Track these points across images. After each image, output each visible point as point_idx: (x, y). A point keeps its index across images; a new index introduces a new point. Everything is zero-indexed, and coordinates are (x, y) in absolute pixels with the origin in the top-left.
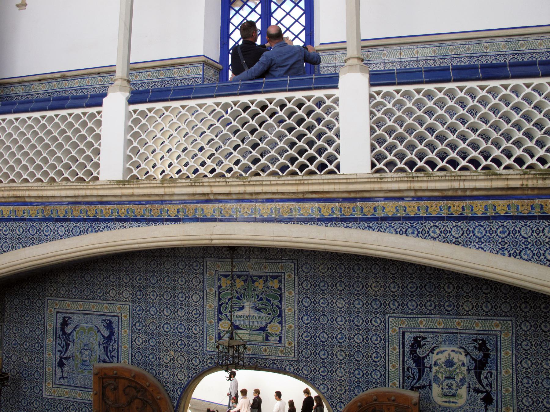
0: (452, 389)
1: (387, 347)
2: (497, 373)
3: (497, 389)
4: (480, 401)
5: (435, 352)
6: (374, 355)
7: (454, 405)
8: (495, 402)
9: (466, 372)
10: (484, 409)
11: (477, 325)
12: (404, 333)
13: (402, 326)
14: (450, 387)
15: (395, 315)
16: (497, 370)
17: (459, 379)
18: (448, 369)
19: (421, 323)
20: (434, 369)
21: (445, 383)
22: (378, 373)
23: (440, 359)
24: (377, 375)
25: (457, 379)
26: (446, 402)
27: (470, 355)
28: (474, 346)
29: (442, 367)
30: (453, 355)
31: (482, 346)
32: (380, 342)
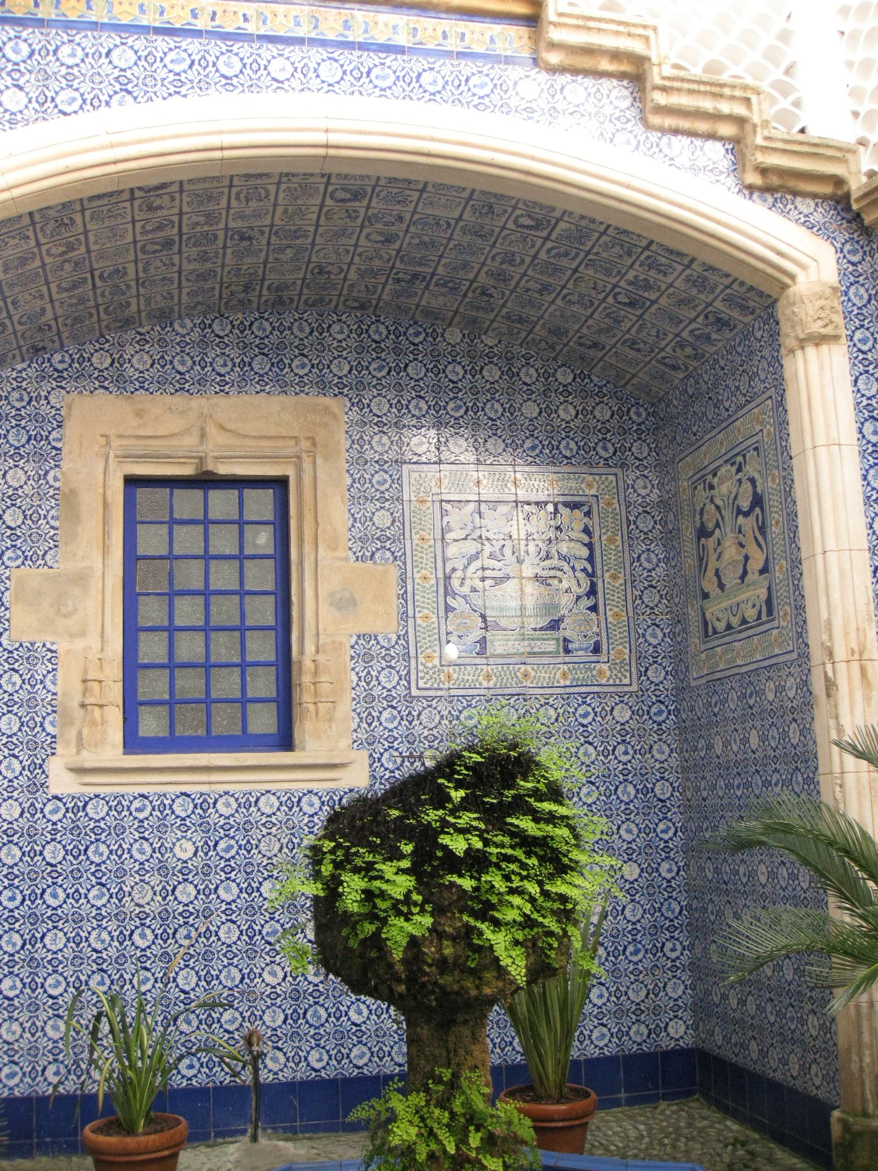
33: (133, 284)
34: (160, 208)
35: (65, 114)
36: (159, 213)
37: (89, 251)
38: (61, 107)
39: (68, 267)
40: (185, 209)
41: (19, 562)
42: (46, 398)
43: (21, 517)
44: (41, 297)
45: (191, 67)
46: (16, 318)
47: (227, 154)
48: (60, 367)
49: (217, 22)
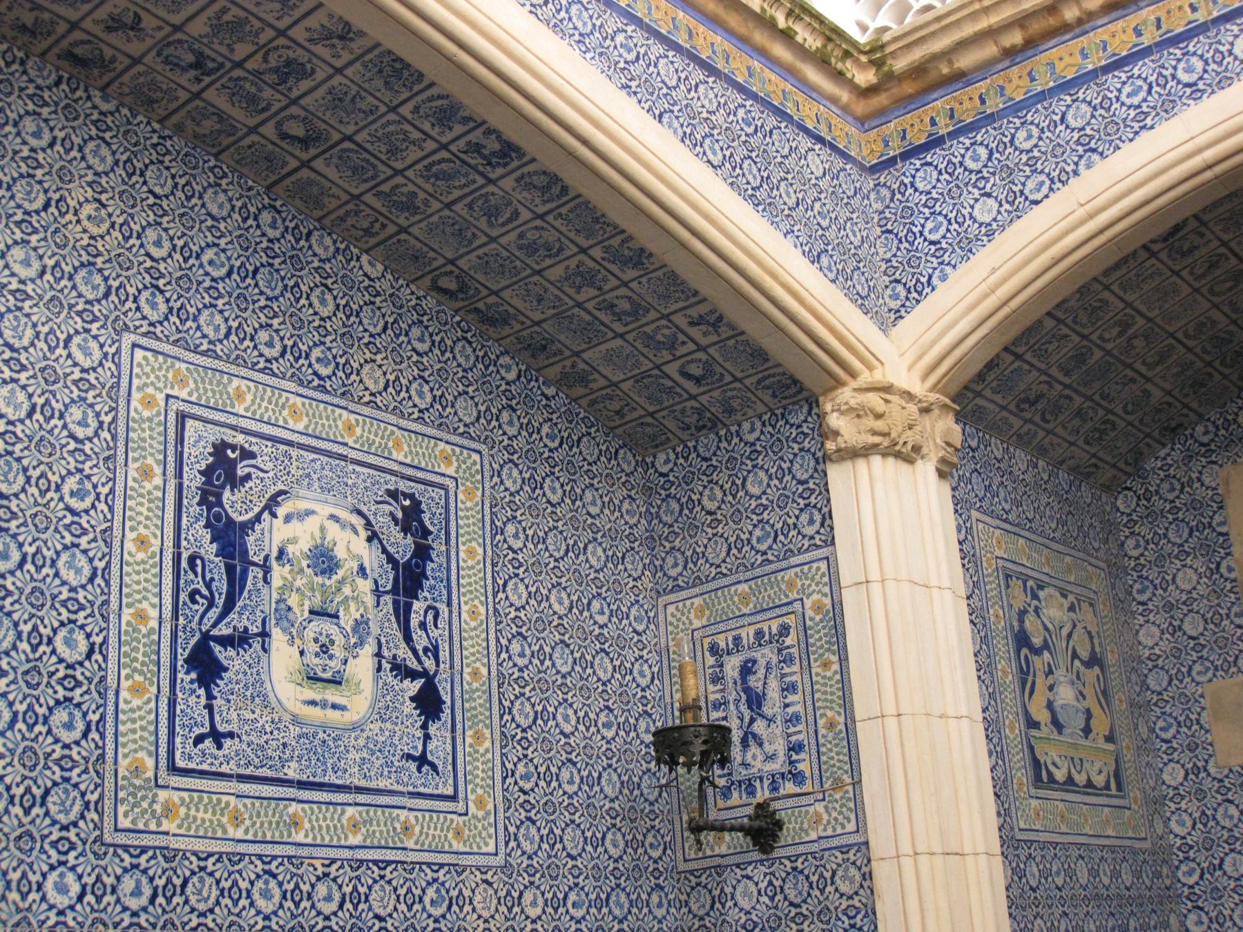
0: (331, 657)
1: (120, 459)
2: (450, 612)
3: (452, 667)
4: (409, 707)
5: (281, 511)
6: (71, 483)
7: (334, 715)
8: (446, 715)
9: (370, 600)
10: (419, 733)
11: (398, 445)
12: (182, 418)
13: (175, 392)
14: (324, 649)
15: (154, 344)
16: (449, 604)
17: (351, 622)
18: (319, 580)
19: (240, 396)
20: (279, 573)
21: (310, 634)
22: (82, 561)
23: (294, 541)
24: (79, 571)
25: (347, 621)
26: (313, 703)
27: (380, 542)
28: (391, 514)
29: (301, 571)
30: (333, 530)
31: (411, 519)
32: (96, 434)
33: (1232, 328)
34: (1193, 249)
35: (1036, 203)
36: (1197, 254)
37: (1150, 320)
38: (1031, 197)
39: (1136, 342)
40: (1226, 237)
41: (1210, 674)
42: (1199, 479)
43: (1202, 623)
44: (1133, 380)
45: (1149, 92)
46: (1119, 410)
47: (1218, 169)
48: (1205, 439)
49: (1164, 28)
